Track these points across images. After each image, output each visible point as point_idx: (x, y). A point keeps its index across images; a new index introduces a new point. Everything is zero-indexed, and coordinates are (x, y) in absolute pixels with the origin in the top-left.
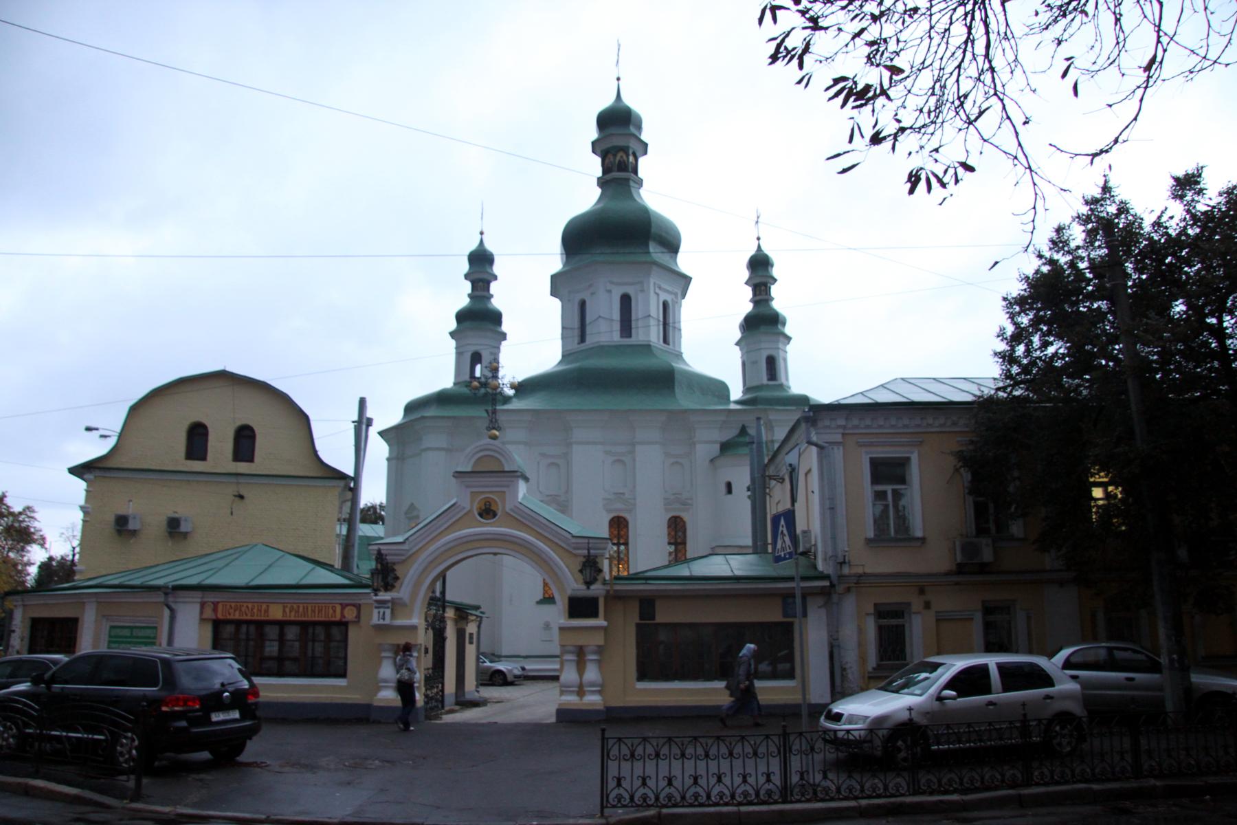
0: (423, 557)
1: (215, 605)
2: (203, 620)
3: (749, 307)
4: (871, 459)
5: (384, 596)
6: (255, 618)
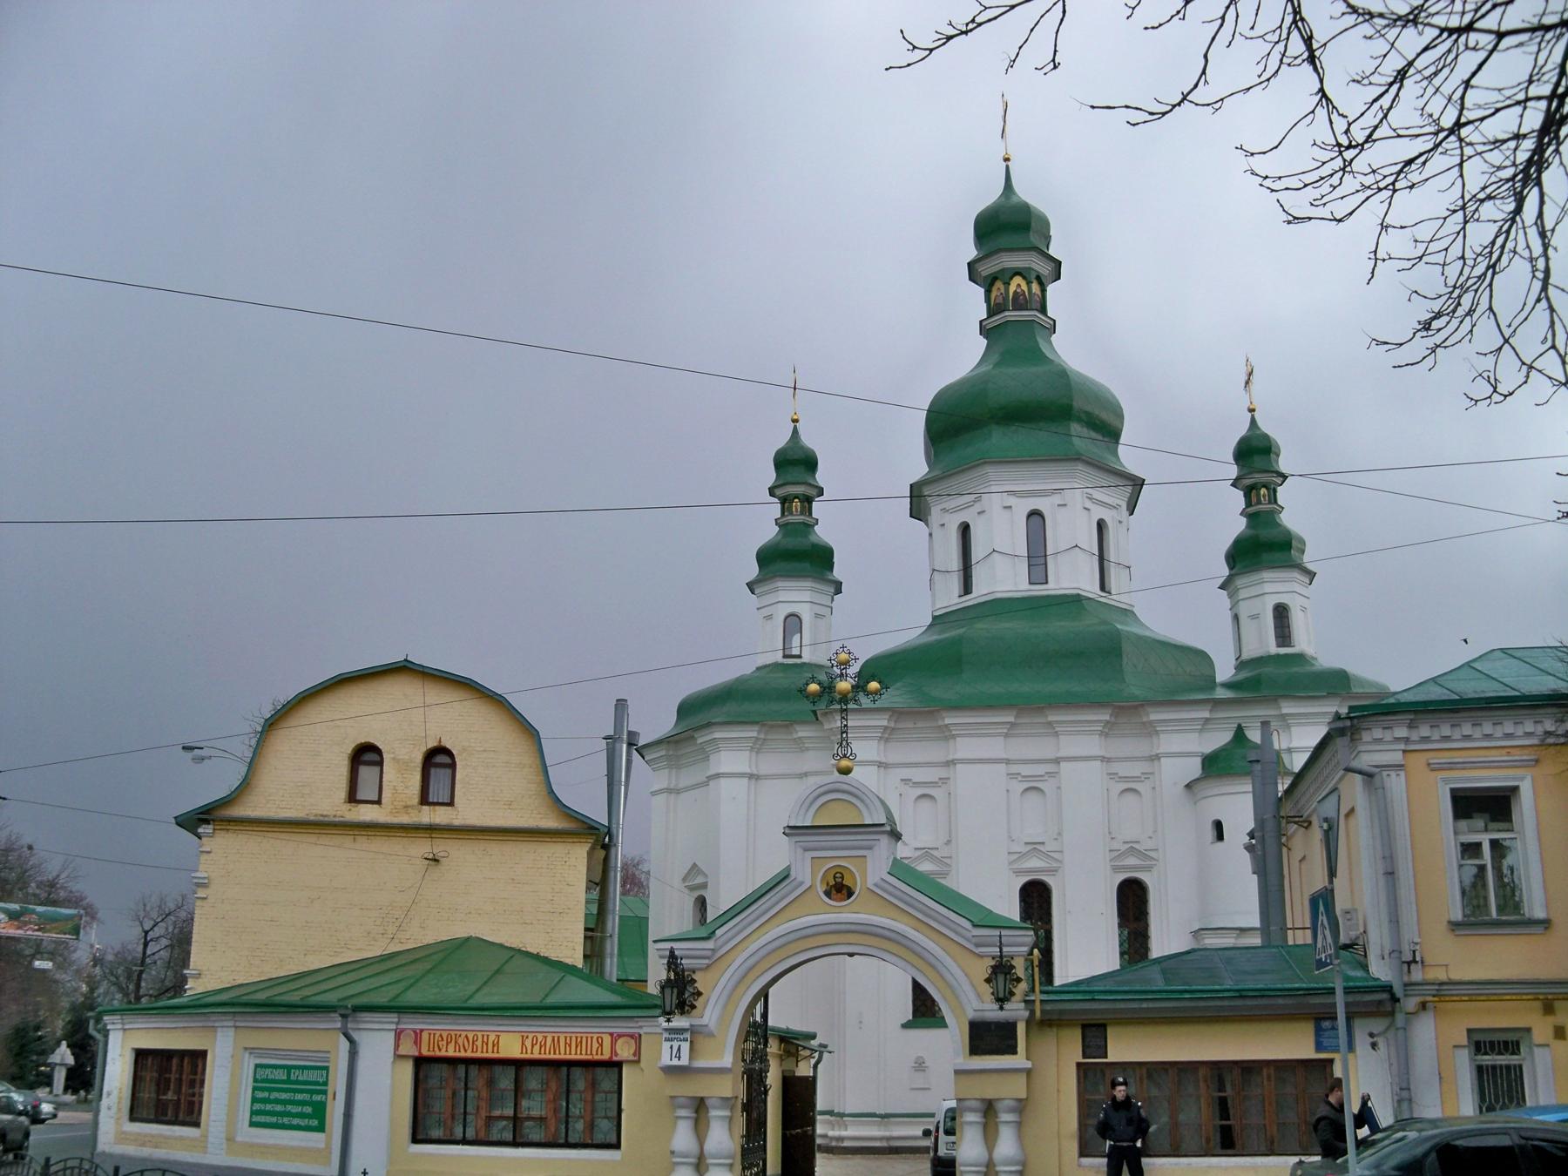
0: (739, 961)
1: (417, 1035)
2: (398, 1057)
3: (1239, 525)
4: (1453, 791)
5: (679, 1022)
6: (479, 1055)
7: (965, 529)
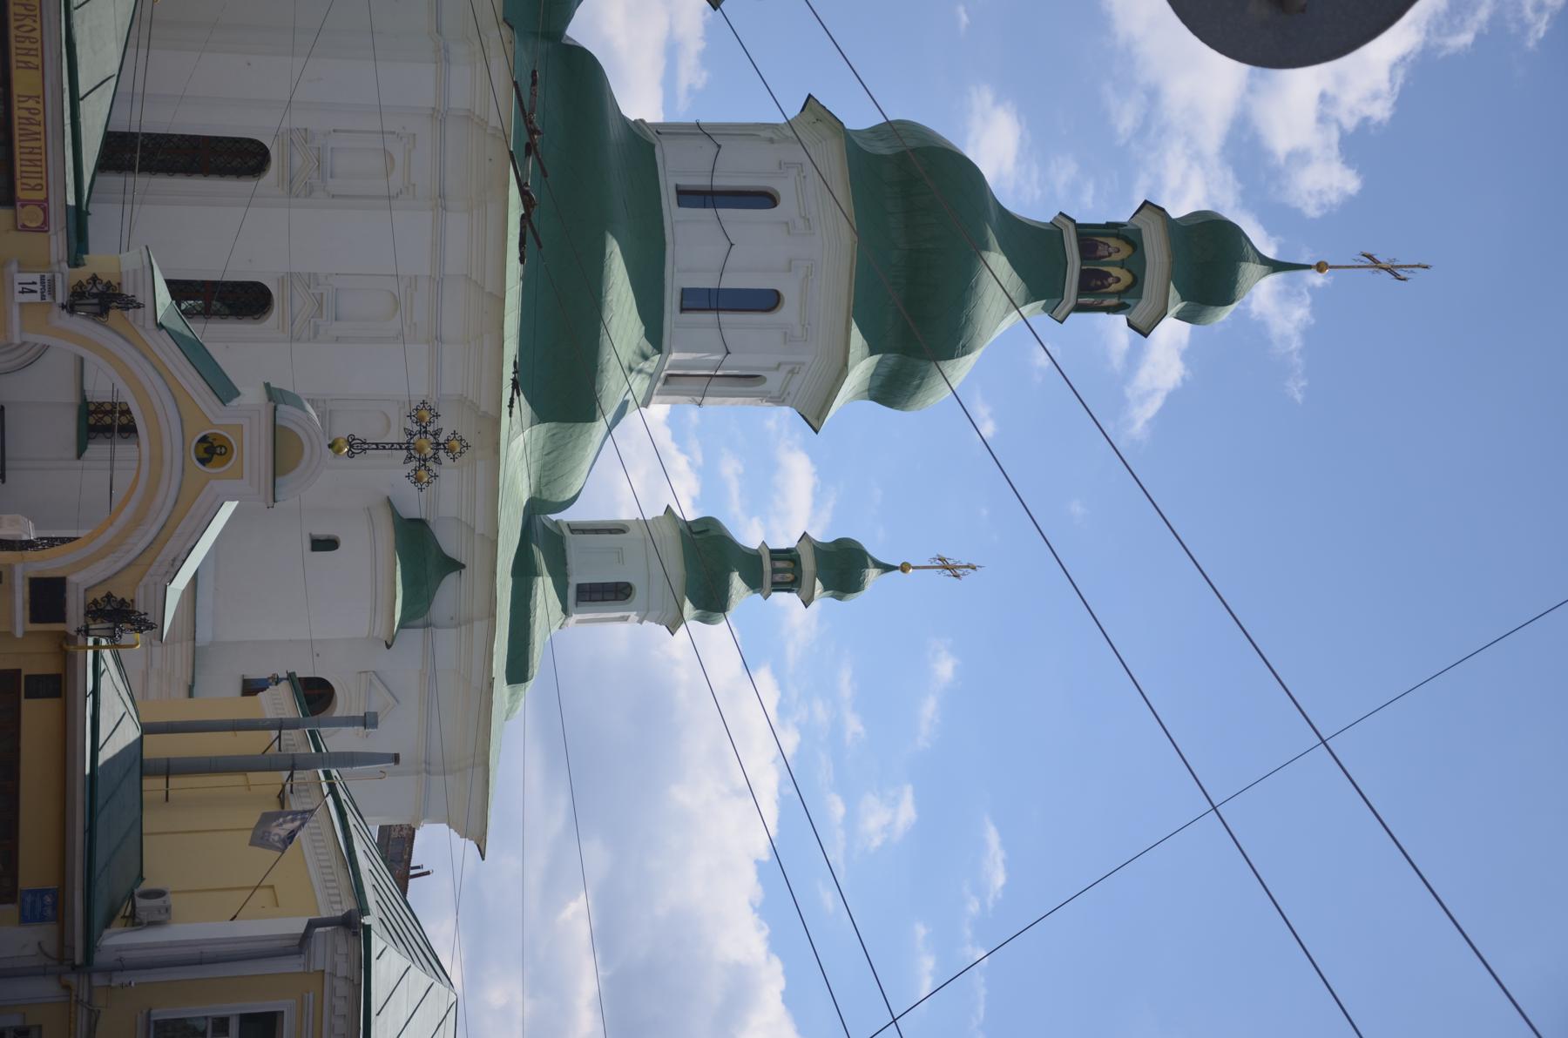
7: (766, 199)
